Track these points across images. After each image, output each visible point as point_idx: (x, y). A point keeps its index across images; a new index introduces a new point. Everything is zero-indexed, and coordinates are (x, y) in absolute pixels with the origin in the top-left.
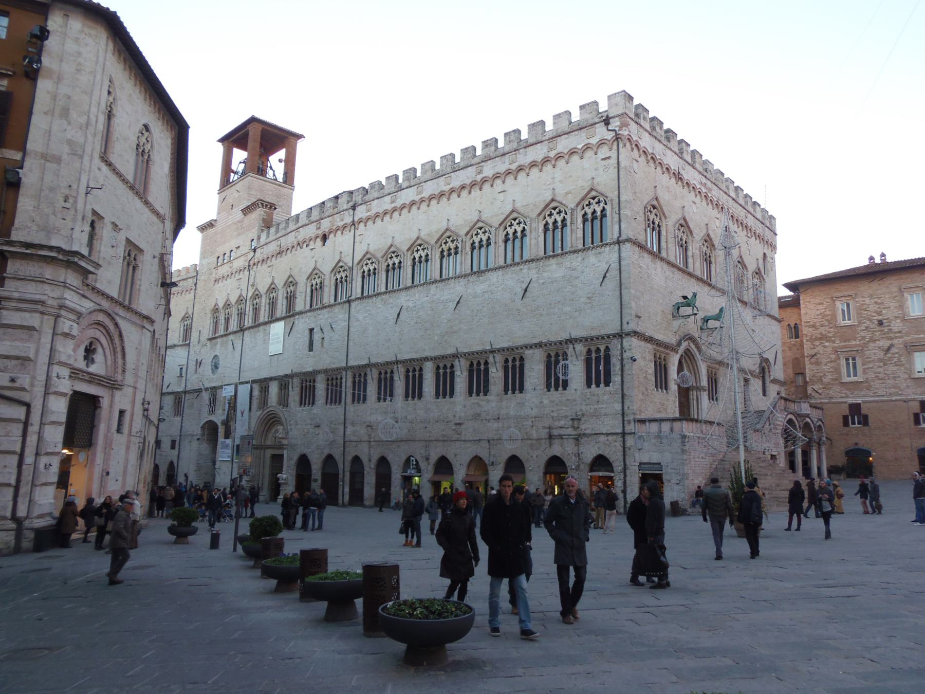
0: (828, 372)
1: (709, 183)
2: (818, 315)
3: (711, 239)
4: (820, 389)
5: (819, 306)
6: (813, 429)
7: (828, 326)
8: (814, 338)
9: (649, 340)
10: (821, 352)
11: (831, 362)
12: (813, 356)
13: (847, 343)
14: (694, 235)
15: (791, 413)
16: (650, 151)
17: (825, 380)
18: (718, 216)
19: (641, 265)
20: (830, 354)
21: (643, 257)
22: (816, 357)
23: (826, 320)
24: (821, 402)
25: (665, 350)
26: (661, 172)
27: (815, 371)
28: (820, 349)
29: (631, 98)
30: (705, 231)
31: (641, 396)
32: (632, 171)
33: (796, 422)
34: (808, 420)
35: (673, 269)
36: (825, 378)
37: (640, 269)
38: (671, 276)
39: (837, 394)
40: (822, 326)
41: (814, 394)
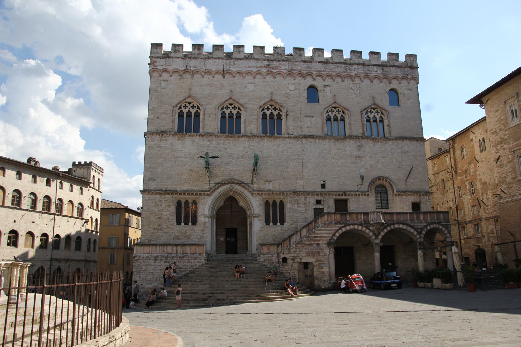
0: (508, 172)
1: (275, 63)
2: (497, 121)
3: (277, 103)
4: (506, 189)
5: (496, 113)
6: (415, 233)
7: (504, 129)
8: (496, 143)
9: (166, 192)
10: (502, 155)
11: (509, 162)
12: (498, 159)
13: (518, 142)
14: (247, 106)
15: (353, 224)
16: (182, 68)
17: (508, 180)
18: (293, 81)
19: (161, 146)
20: (508, 155)
21: (165, 140)
22: (500, 160)
23: (502, 124)
24: (507, 201)
25: (192, 196)
26: (201, 76)
27: (501, 173)
28: (501, 152)
29: (160, 45)
30: (269, 99)
31: (151, 230)
32: (159, 89)
33: (368, 231)
34: (401, 226)
35: (210, 138)
36: (508, 178)
37: (159, 149)
38: (208, 143)
39: (517, 191)
40: (501, 130)
41: (503, 195)
